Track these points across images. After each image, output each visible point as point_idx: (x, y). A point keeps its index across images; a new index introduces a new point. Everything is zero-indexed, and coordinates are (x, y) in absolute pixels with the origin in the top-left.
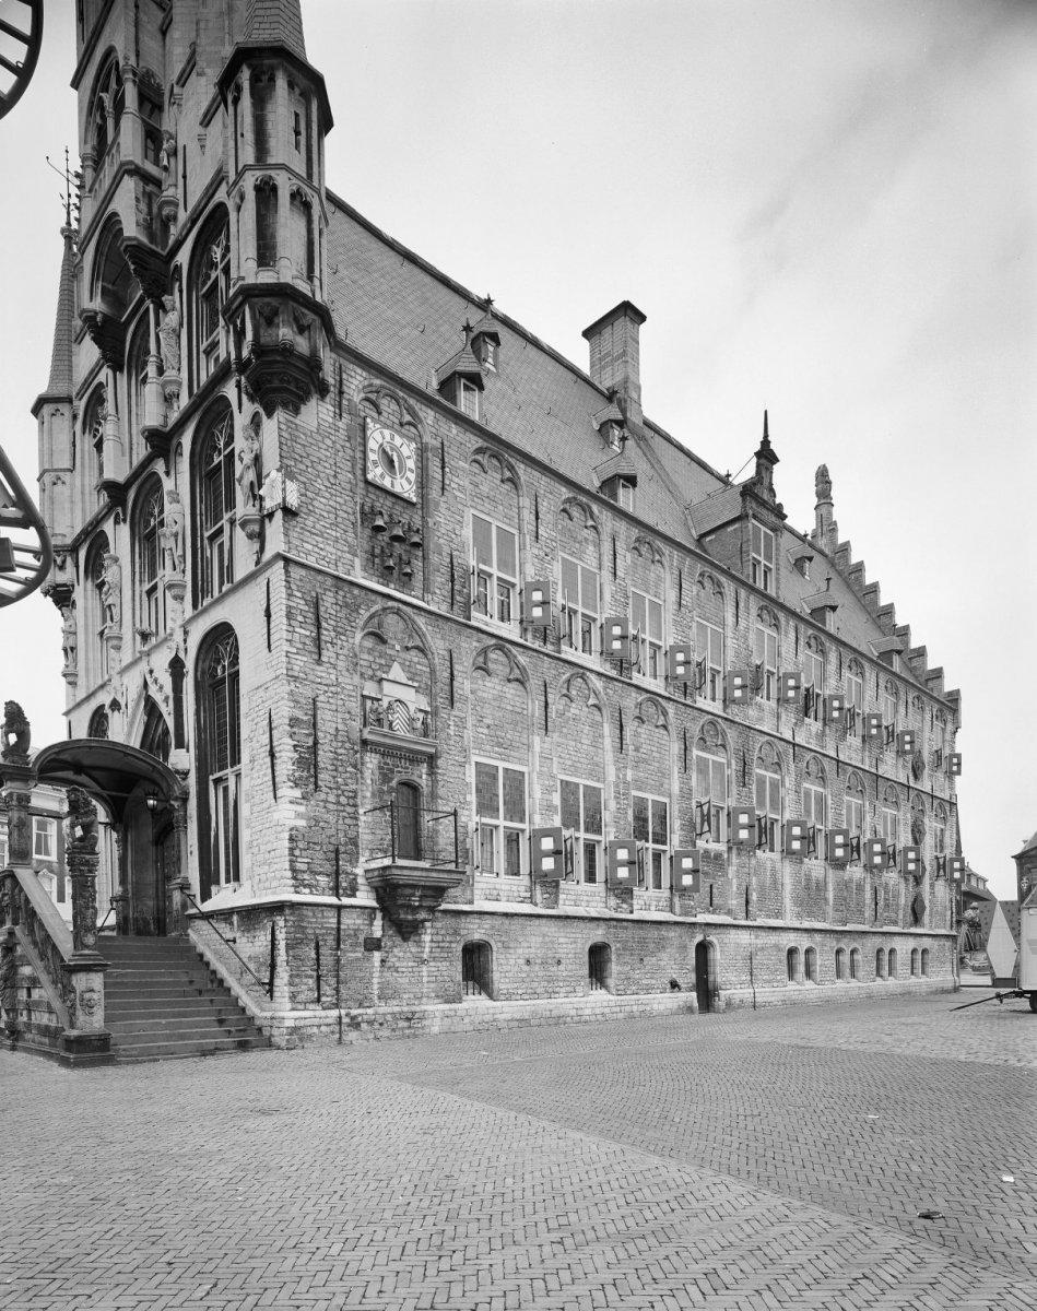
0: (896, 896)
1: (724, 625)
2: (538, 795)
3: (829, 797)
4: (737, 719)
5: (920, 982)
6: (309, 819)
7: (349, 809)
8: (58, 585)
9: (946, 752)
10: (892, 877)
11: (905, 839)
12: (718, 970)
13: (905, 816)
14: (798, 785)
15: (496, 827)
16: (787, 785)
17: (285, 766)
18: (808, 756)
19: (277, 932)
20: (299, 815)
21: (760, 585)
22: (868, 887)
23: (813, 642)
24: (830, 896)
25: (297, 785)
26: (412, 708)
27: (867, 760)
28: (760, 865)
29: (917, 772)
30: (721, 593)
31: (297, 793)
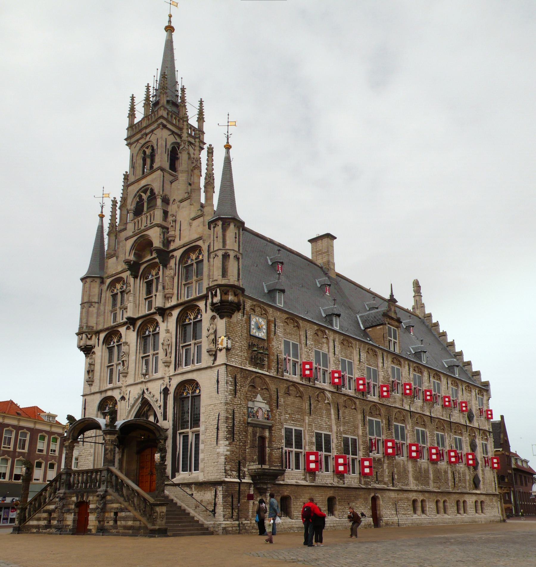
0: (464, 475)
1: (378, 367)
2: (307, 438)
3: (428, 433)
4: (385, 403)
5: (481, 517)
6: (230, 451)
7: (243, 447)
8: (87, 346)
9: (485, 408)
10: (461, 467)
11: (466, 449)
12: (381, 509)
13: (466, 440)
14: (413, 428)
15: (292, 451)
16: (408, 428)
17: (222, 434)
18: (417, 416)
19: (218, 492)
20: (228, 451)
21: (392, 349)
22: (449, 472)
23: (416, 369)
24: (431, 476)
25: (227, 440)
26: (264, 410)
27: (445, 416)
28: (398, 463)
29: (470, 418)
30: (376, 355)
31: (227, 442)
